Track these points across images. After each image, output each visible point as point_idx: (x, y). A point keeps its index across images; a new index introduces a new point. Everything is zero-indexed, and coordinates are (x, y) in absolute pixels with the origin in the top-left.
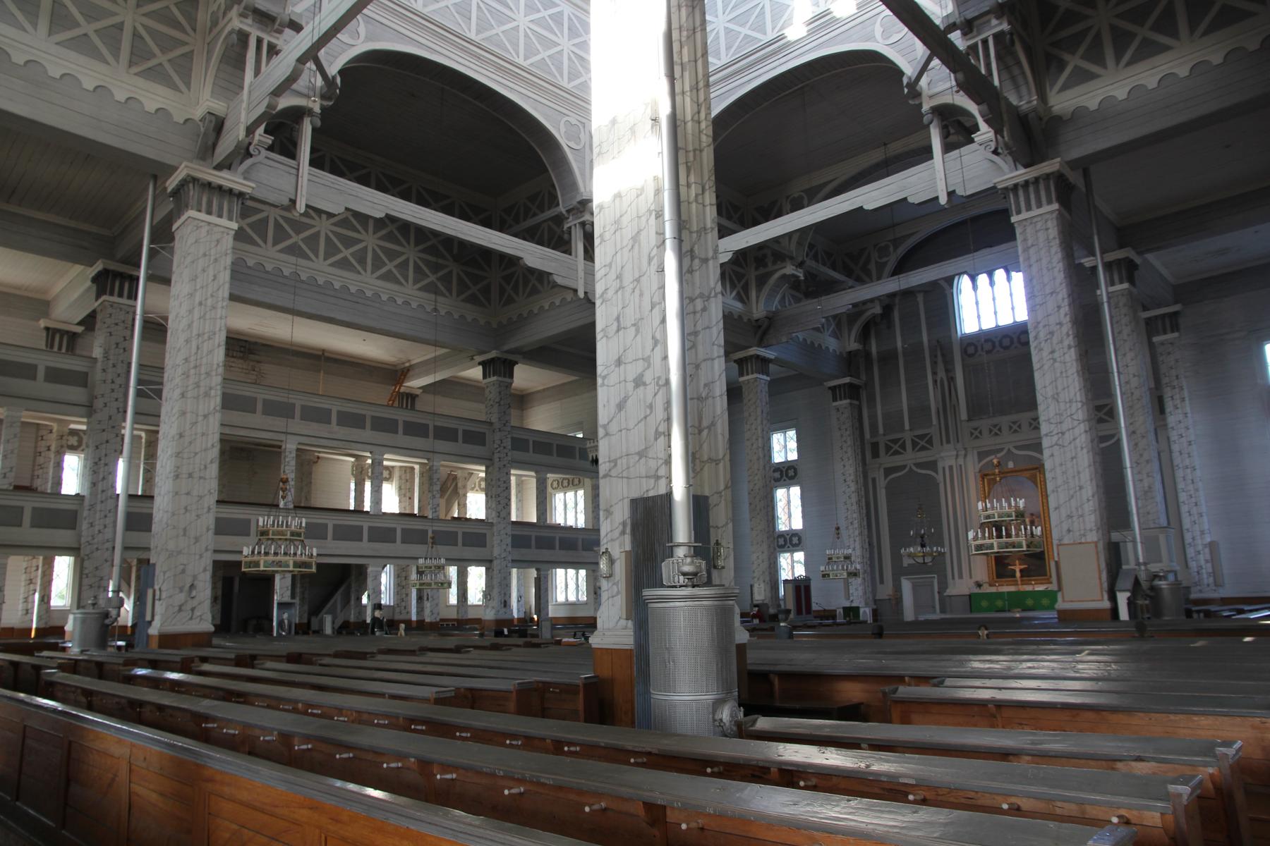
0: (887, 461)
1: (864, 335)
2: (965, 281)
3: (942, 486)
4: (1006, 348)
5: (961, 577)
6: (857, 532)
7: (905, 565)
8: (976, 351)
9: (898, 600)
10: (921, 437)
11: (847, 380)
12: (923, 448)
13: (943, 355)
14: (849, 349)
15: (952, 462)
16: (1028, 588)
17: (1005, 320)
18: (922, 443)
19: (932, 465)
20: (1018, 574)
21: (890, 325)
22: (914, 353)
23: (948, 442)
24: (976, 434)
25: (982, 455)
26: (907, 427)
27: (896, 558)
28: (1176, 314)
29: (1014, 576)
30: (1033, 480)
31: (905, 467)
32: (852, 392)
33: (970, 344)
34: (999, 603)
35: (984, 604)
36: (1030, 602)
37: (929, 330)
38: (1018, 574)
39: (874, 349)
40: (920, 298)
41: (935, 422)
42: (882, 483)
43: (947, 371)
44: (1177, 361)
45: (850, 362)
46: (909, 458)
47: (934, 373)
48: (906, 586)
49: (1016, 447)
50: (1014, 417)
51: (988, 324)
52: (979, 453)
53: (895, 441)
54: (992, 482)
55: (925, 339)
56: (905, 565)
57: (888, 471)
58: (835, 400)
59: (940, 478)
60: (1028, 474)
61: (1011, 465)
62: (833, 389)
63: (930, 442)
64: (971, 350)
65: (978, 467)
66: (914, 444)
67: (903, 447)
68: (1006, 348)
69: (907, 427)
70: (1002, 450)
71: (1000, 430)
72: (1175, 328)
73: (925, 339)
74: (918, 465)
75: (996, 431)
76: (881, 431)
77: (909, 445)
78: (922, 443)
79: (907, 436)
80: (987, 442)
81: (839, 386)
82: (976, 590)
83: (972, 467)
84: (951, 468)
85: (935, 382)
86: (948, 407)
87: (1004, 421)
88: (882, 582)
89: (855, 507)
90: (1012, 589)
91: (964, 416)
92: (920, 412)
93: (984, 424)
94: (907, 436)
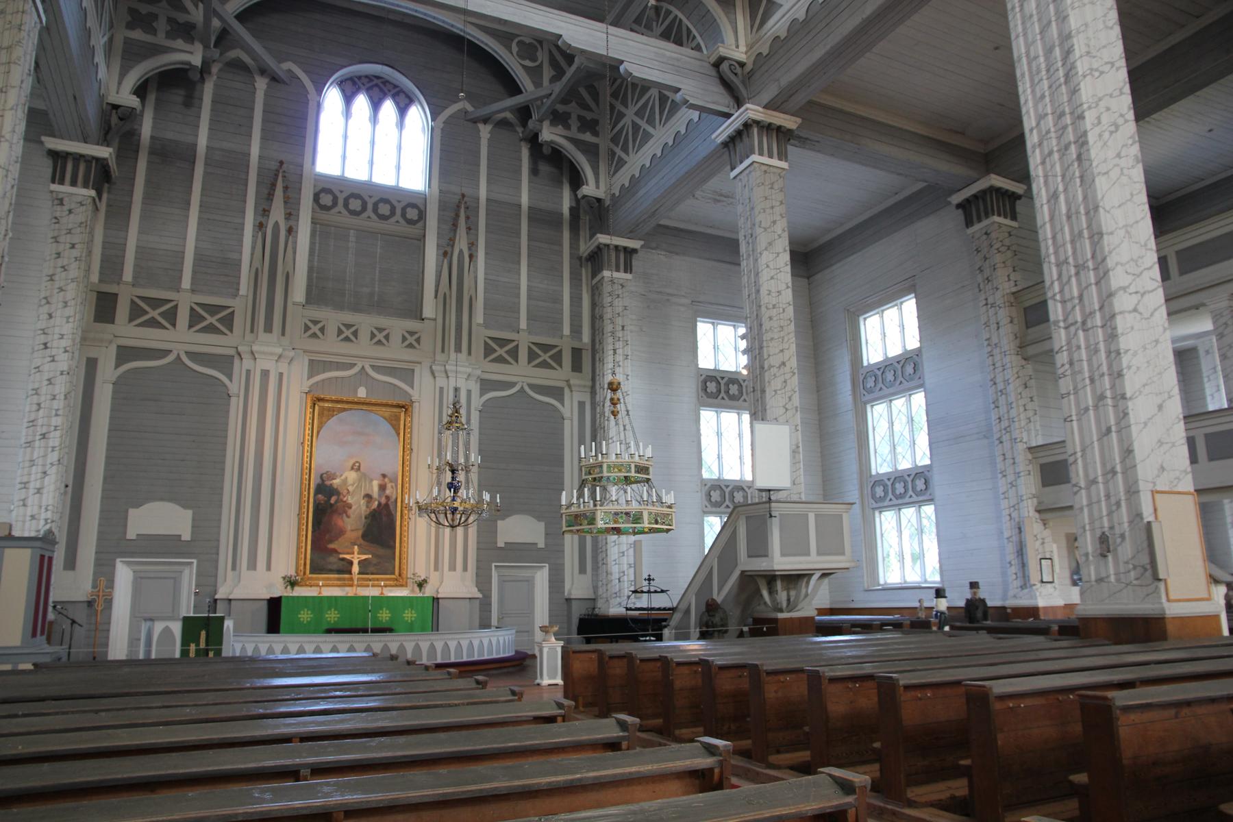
0: (126, 331)
1: (141, 91)
2: (332, 97)
3: (236, 405)
4: (383, 218)
5: (252, 566)
6: (54, 457)
7: (131, 534)
8: (335, 203)
9: (98, 605)
10: (213, 309)
11: (104, 152)
12: (211, 329)
13: (286, 188)
14: (113, 98)
15: (263, 364)
16: (372, 592)
17: (384, 177)
18: (211, 320)
19: (225, 363)
20: (356, 568)
21: (191, 101)
22: (228, 167)
23: (268, 329)
24: (315, 330)
25: (315, 367)
26: (186, 283)
27: (113, 518)
28: (634, 251)
29: (350, 573)
30: (394, 422)
31: (167, 352)
32: (101, 177)
33: (327, 191)
34: (332, 617)
35: (305, 616)
36: (384, 616)
37: (264, 139)
38: (356, 568)
39: (146, 129)
40: (261, 84)
41: (243, 290)
42: (108, 372)
43: (288, 216)
44: (625, 308)
45: (116, 125)
46: (180, 339)
47: (264, 212)
48: (124, 574)
49: (373, 367)
50: (382, 321)
51: (357, 172)
52: (311, 362)
53: (155, 303)
54: (326, 415)
55: (255, 151)
56: (131, 534)
57: (125, 354)
58: (57, 177)
59: (234, 387)
60: (388, 412)
61: (362, 393)
62: (55, 155)
63: (229, 321)
64: (326, 200)
65: (306, 385)
66: (195, 318)
67: (171, 316)
68: (383, 218)
69: (186, 283)
70: (353, 365)
71: (355, 334)
72: (628, 268)
73: (255, 151)
74: (192, 355)
75: (348, 334)
76: (128, 275)
77: (183, 317)
78: (211, 320)
79: (185, 302)
80: (331, 346)
81: (78, 158)
83: (297, 384)
84: (265, 374)
85: (260, 226)
86: (272, 272)
87: (366, 322)
88: (71, 564)
89: (59, 404)
90: (349, 592)
91: (299, 293)
92: (218, 267)
93: (332, 318)
94: (185, 302)
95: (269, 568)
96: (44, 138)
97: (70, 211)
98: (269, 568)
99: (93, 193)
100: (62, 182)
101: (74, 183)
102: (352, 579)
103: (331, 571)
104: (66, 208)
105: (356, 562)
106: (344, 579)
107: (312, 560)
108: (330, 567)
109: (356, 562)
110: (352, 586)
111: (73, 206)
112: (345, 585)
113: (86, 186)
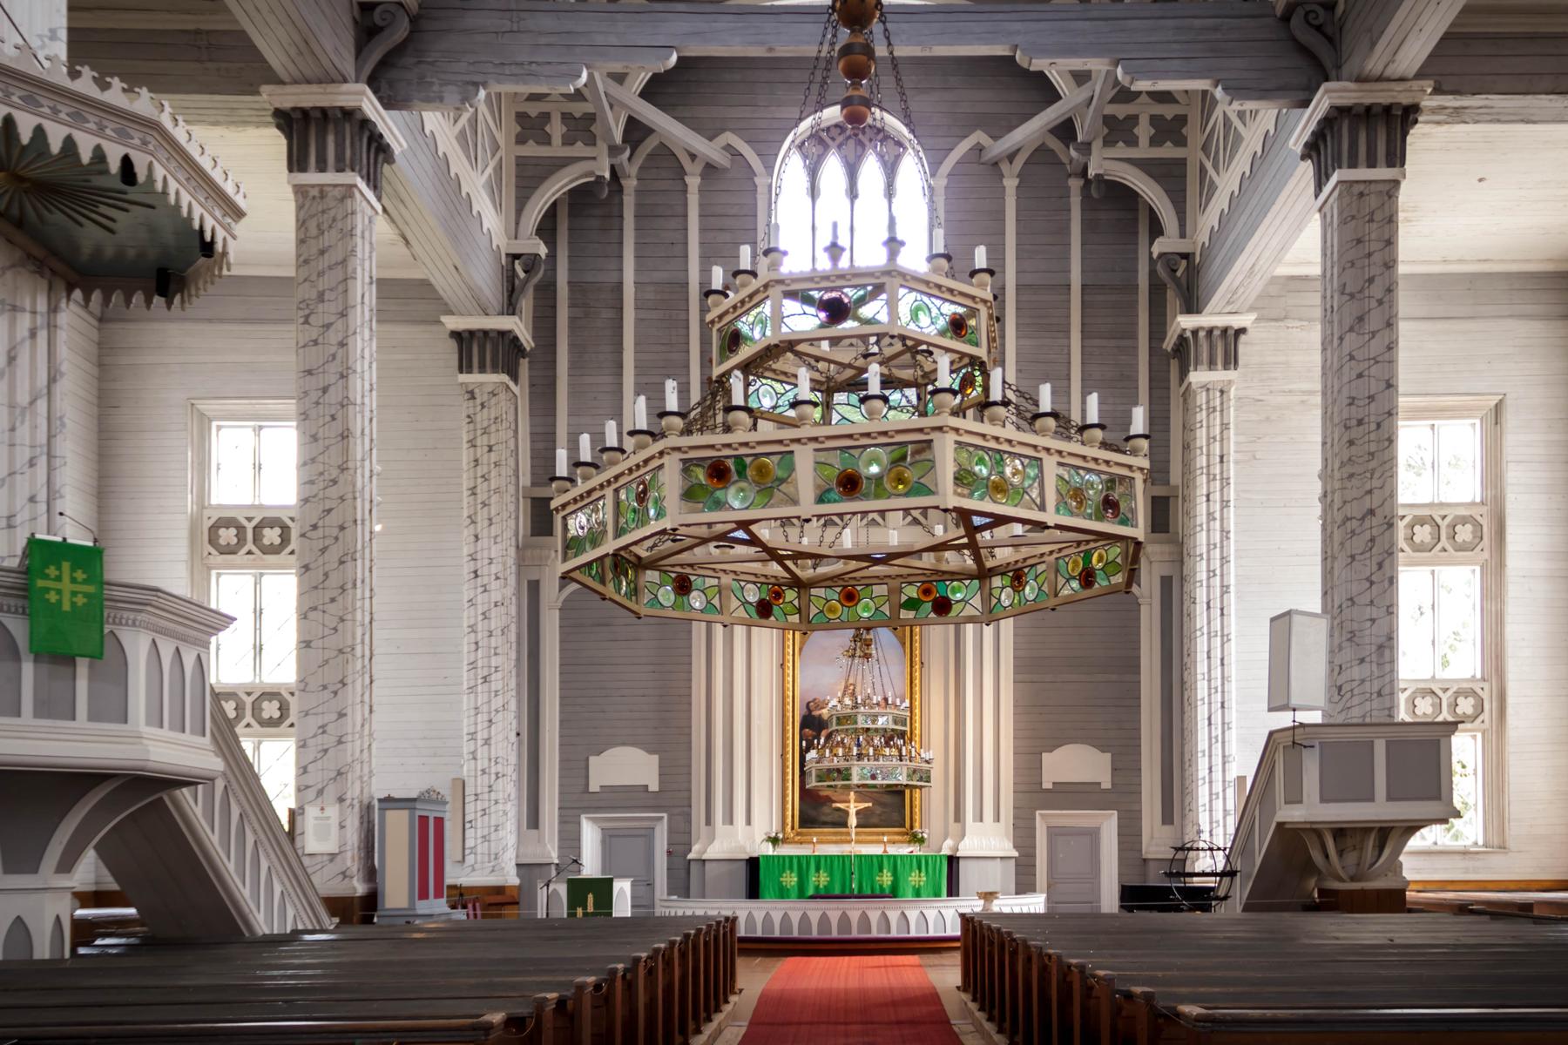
58: (465, 366)
82: (768, 850)
90: (845, 849)
95: (749, 822)
96: (444, 319)
97: (482, 405)
98: (749, 822)
99: (505, 378)
100: (470, 371)
101: (482, 369)
102: (849, 834)
103: (825, 824)
104: (478, 401)
105: (853, 811)
106: (841, 834)
107: (801, 811)
108: (824, 818)
109: (853, 811)
110: (850, 842)
111: (485, 397)
112: (842, 842)
113: (495, 370)
